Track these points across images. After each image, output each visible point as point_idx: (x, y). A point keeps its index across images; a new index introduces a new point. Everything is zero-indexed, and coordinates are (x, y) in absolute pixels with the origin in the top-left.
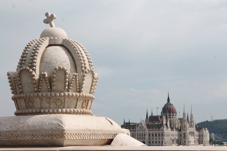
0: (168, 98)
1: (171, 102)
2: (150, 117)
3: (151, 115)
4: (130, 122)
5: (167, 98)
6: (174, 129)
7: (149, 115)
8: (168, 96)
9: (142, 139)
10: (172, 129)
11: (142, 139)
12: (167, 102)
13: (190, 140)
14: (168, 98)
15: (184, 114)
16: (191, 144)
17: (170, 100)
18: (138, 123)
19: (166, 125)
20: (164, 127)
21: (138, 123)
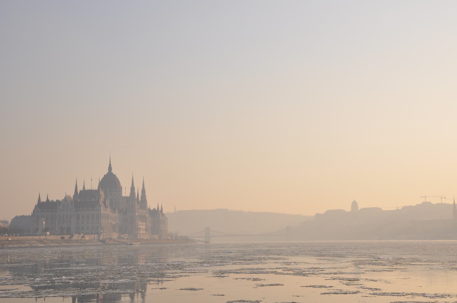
0: (110, 165)
1: (114, 171)
2: (80, 191)
3: (82, 189)
4: (49, 198)
5: (108, 166)
6: (117, 211)
7: (80, 188)
8: (109, 164)
9: (67, 223)
10: (113, 210)
11: (67, 223)
12: (108, 171)
13: (139, 227)
14: (110, 165)
15: (133, 189)
16: (141, 232)
17: (113, 169)
18: (61, 200)
19: (104, 202)
20: (100, 206)
21: (61, 200)
